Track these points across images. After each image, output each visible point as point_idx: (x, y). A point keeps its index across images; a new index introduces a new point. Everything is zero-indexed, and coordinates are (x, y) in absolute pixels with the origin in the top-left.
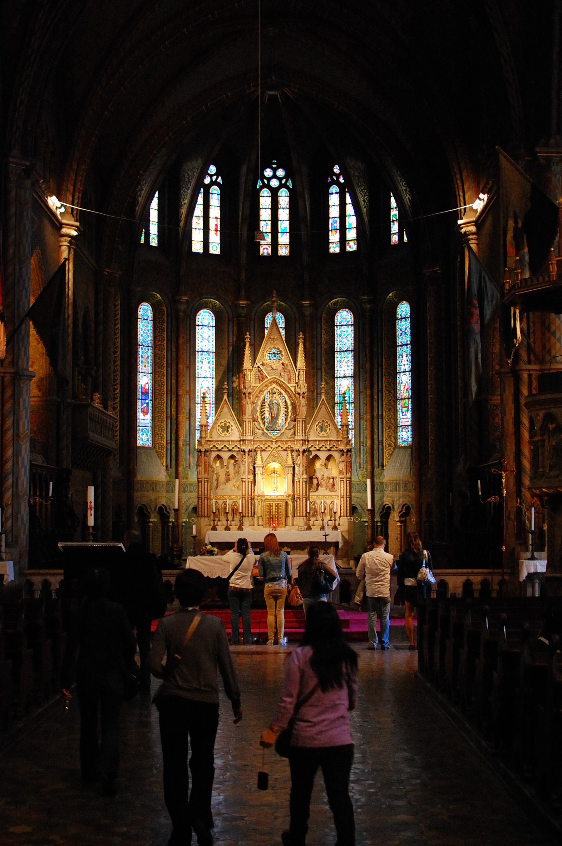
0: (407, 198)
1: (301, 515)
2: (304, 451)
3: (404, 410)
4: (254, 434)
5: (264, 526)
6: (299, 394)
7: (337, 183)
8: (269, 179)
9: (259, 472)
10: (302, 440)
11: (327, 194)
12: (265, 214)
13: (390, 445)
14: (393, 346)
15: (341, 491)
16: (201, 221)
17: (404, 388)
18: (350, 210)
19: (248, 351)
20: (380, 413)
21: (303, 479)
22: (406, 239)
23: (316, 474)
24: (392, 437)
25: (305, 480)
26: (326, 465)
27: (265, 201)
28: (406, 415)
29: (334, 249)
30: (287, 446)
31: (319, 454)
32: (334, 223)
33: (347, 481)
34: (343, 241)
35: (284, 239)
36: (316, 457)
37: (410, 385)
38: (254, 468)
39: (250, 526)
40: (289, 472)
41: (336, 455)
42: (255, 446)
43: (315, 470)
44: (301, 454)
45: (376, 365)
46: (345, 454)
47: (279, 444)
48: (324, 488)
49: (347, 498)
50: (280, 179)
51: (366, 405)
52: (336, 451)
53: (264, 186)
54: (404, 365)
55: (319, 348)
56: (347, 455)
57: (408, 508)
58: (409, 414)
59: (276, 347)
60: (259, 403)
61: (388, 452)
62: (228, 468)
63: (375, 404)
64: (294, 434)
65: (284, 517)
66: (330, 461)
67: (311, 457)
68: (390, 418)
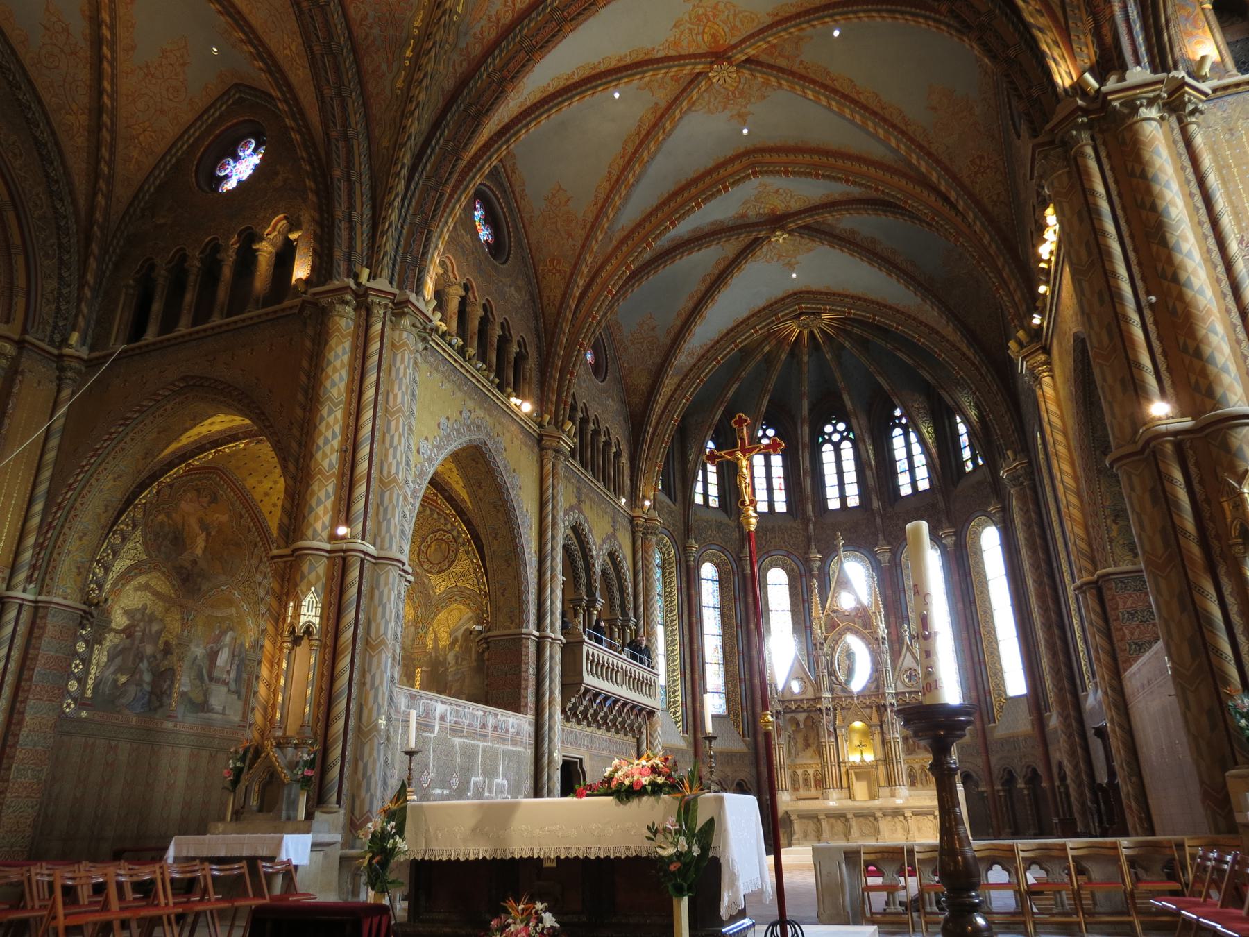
0: (973, 413)
7: (900, 425)
8: (830, 435)
11: (890, 438)
16: (764, 481)
18: (916, 448)
19: (816, 599)
22: (981, 462)
27: (828, 453)
29: (906, 490)
32: (902, 465)
34: (914, 483)
35: (852, 491)
38: (835, 729)
50: (841, 433)
53: (825, 441)
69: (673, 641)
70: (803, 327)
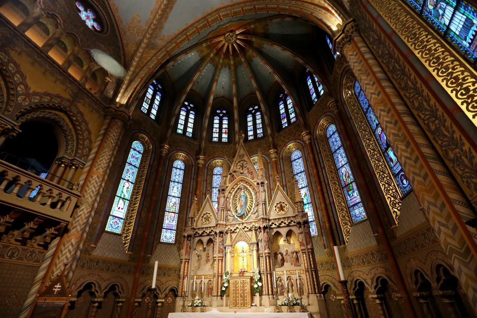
1: (267, 293)
2: (265, 228)
3: (350, 193)
4: (227, 220)
5: (231, 306)
6: (258, 184)
9: (229, 251)
10: (263, 219)
12: (250, 124)
13: (346, 224)
14: (331, 154)
15: (305, 264)
17: (346, 177)
20: (331, 200)
21: (265, 254)
23: (281, 250)
24: (346, 217)
25: (267, 255)
26: (288, 242)
28: (353, 195)
30: (251, 226)
31: (280, 230)
33: (309, 252)
36: (278, 234)
37: (350, 172)
39: (218, 306)
40: (254, 249)
41: (295, 229)
42: (227, 229)
43: (279, 246)
44: (262, 231)
45: (320, 170)
46: (302, 226)
47: (245, 225)
48: (289, 264)
49: (312, 271)
51: (319, 198)
52: (294, 225)
54: (341, 161)
55: (283, 174)
56: (305, 227)
57: (384, 282)
58: (356, 194)
59: (243, 159)
60: (232, 197)
61: (347, 230)
62: (208, 250)
63: (326, 195)
64: (258, 216)
65: (250, 296)
66: (292, 237)
67: (273, 234)
68: (341, 202)
69: (137, 193)
70: (228, 41)
